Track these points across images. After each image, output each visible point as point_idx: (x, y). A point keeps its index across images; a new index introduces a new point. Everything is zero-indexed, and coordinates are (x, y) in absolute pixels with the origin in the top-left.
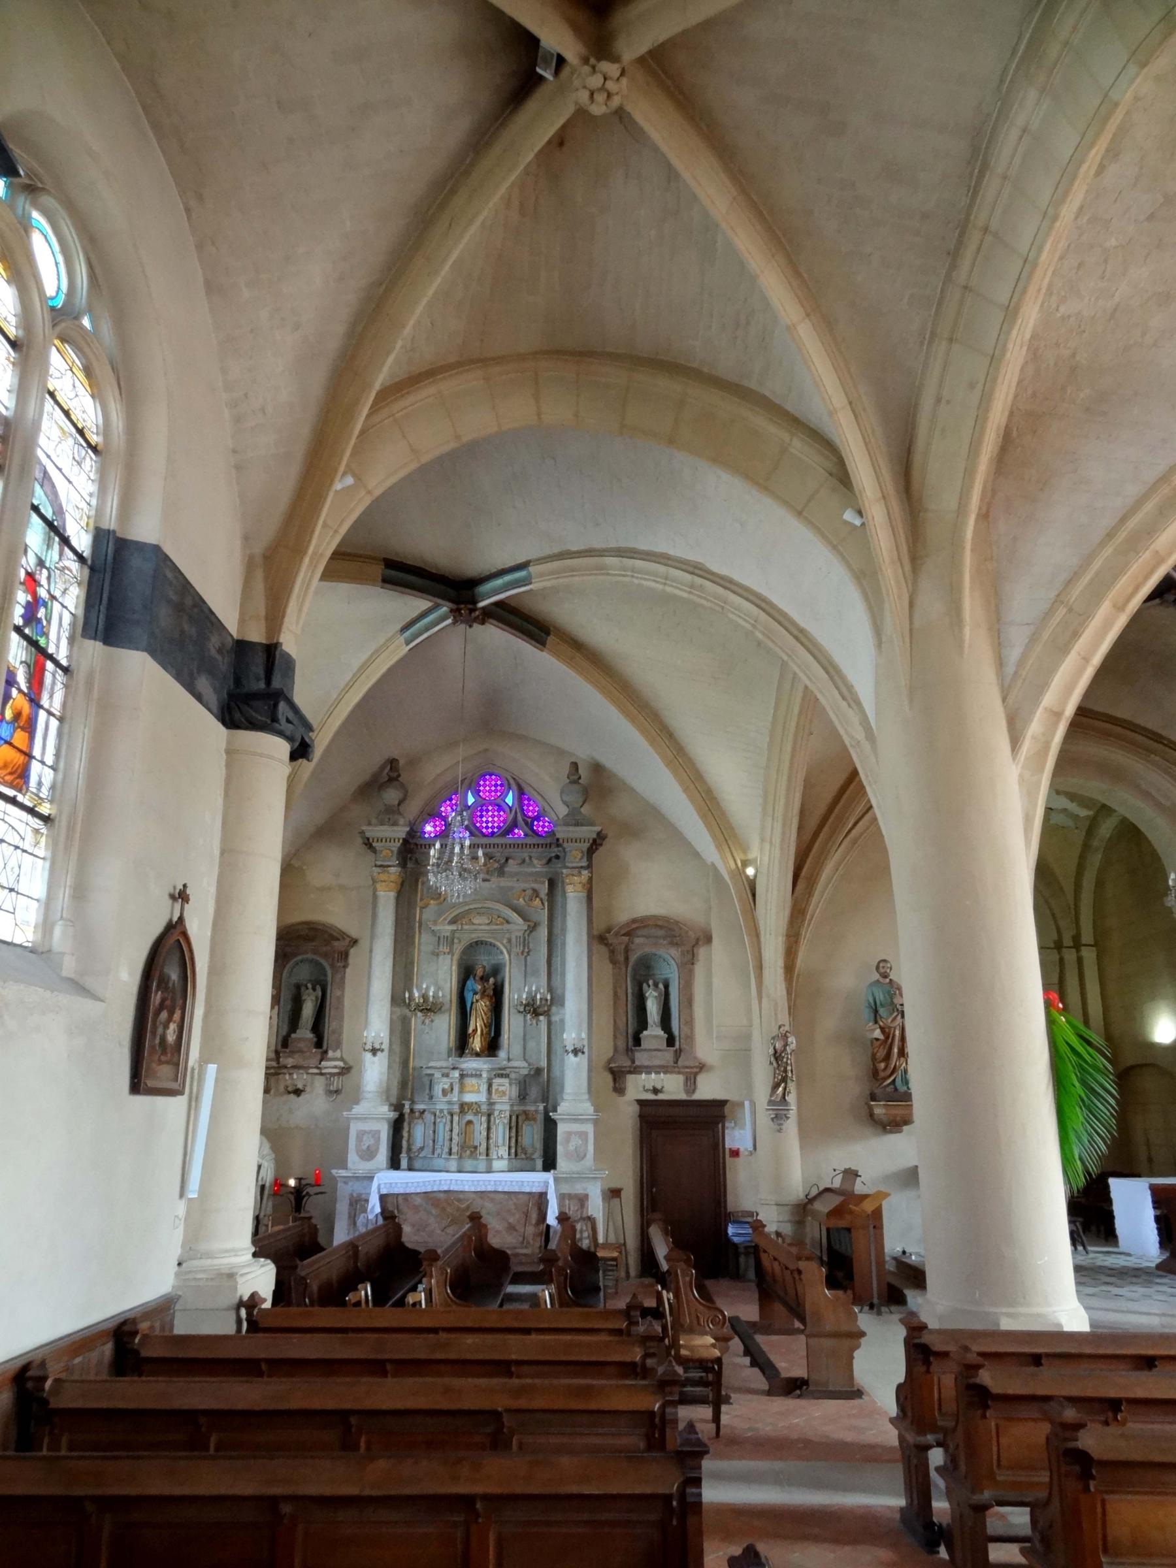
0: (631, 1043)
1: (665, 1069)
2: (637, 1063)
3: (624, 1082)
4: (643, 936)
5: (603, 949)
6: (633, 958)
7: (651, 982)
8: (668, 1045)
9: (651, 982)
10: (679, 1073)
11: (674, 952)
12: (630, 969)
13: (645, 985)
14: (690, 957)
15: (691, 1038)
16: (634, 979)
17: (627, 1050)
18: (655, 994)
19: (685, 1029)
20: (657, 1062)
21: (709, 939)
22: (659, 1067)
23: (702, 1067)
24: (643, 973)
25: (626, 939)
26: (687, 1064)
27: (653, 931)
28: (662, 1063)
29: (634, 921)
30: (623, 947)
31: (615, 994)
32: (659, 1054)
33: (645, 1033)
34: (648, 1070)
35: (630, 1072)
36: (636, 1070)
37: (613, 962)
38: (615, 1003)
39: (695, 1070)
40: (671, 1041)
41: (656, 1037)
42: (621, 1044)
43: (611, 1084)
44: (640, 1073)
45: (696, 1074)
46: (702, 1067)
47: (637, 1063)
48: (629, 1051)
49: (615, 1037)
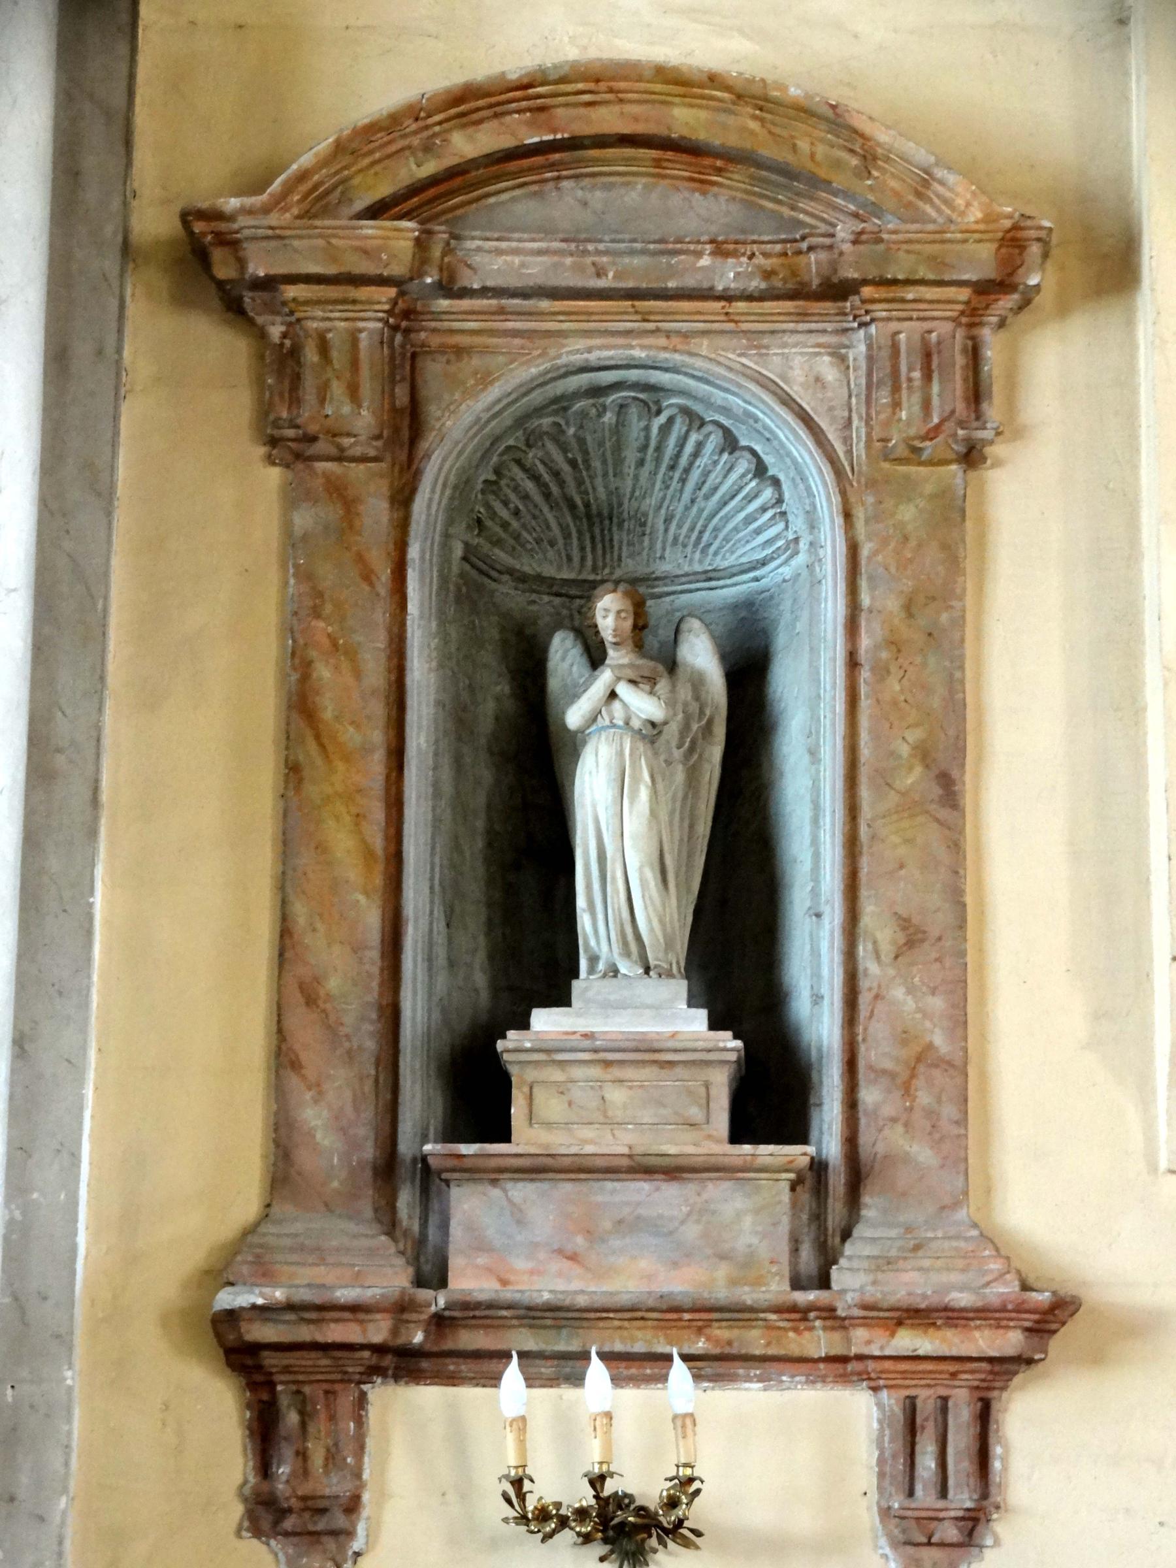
0: (419, 1099)
1: (717, 1340)
2: (468, 1280)
3: (348, 1454)
4: (546, 230)
5: (218, 347)
6: (461, 421)
7: (609, 613)
8: (743, 1129)
9: (609, 613)
10: (842, 1367)
11: (809, 362)
12: (428, 502)
13: (563, 654)
14: (947, 394)
15: (948, 1074)
16: (470, 586)
17: (387, 1169)
18: (642, 705)
19: (903, 998)
20: (636, 1273)
21: (1112, 266)
22: (671, 1313)
23: (1046, 1319)
24: (546, 541)
25: (396, 240)
26: (911, 1284)
27: (639, 198)
28: (682, 1283)
29: (469, 103)
30: (366, 321)
31: (300, 705)
32: (667, 1199)
33: (544, 1020)
34: (558, 1339)
35: (404, 1364)
36: (443, 1346)
37: (288, 442)
38: (293, 772)
39: (985, 1342)
40: (770, 1097)
41: (649, 1053)
42: (333, 1126)
43: (233, 1464)
44: (484, 1367)
45: (1005, 1369)
46: (1046, 1319)
47: (468, 1280)
48: (401, 1186)
49: (284, 1059)
